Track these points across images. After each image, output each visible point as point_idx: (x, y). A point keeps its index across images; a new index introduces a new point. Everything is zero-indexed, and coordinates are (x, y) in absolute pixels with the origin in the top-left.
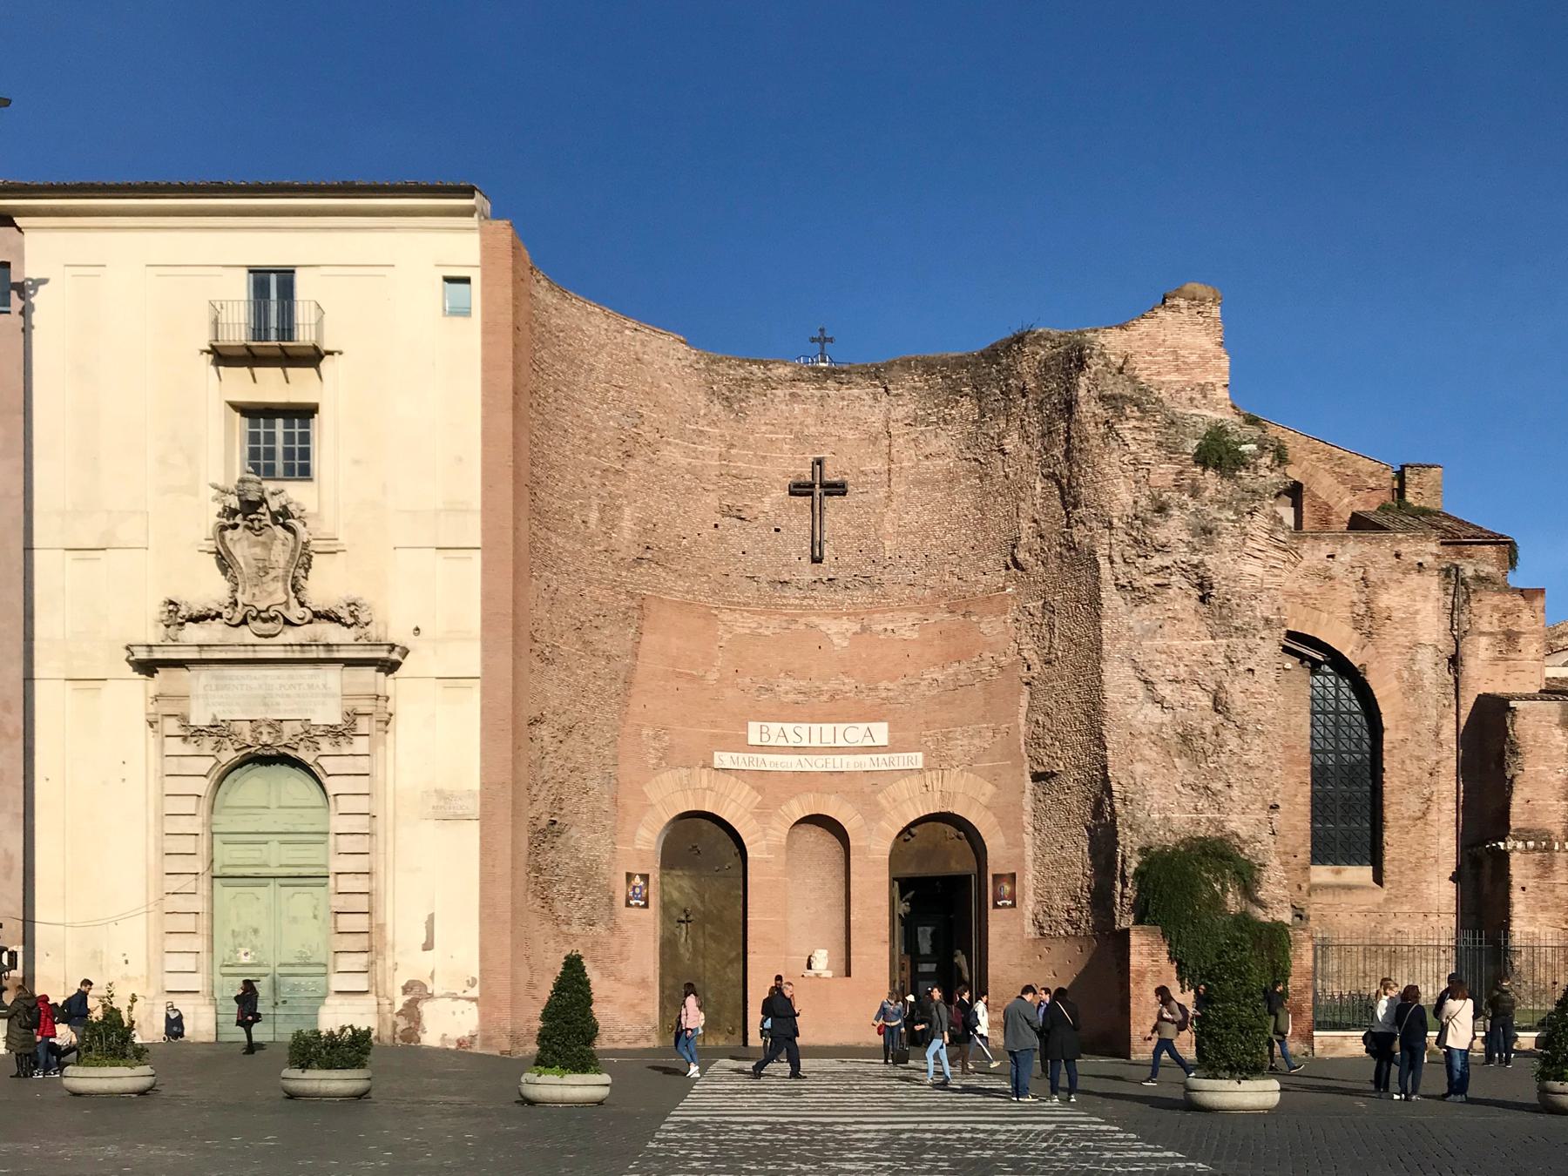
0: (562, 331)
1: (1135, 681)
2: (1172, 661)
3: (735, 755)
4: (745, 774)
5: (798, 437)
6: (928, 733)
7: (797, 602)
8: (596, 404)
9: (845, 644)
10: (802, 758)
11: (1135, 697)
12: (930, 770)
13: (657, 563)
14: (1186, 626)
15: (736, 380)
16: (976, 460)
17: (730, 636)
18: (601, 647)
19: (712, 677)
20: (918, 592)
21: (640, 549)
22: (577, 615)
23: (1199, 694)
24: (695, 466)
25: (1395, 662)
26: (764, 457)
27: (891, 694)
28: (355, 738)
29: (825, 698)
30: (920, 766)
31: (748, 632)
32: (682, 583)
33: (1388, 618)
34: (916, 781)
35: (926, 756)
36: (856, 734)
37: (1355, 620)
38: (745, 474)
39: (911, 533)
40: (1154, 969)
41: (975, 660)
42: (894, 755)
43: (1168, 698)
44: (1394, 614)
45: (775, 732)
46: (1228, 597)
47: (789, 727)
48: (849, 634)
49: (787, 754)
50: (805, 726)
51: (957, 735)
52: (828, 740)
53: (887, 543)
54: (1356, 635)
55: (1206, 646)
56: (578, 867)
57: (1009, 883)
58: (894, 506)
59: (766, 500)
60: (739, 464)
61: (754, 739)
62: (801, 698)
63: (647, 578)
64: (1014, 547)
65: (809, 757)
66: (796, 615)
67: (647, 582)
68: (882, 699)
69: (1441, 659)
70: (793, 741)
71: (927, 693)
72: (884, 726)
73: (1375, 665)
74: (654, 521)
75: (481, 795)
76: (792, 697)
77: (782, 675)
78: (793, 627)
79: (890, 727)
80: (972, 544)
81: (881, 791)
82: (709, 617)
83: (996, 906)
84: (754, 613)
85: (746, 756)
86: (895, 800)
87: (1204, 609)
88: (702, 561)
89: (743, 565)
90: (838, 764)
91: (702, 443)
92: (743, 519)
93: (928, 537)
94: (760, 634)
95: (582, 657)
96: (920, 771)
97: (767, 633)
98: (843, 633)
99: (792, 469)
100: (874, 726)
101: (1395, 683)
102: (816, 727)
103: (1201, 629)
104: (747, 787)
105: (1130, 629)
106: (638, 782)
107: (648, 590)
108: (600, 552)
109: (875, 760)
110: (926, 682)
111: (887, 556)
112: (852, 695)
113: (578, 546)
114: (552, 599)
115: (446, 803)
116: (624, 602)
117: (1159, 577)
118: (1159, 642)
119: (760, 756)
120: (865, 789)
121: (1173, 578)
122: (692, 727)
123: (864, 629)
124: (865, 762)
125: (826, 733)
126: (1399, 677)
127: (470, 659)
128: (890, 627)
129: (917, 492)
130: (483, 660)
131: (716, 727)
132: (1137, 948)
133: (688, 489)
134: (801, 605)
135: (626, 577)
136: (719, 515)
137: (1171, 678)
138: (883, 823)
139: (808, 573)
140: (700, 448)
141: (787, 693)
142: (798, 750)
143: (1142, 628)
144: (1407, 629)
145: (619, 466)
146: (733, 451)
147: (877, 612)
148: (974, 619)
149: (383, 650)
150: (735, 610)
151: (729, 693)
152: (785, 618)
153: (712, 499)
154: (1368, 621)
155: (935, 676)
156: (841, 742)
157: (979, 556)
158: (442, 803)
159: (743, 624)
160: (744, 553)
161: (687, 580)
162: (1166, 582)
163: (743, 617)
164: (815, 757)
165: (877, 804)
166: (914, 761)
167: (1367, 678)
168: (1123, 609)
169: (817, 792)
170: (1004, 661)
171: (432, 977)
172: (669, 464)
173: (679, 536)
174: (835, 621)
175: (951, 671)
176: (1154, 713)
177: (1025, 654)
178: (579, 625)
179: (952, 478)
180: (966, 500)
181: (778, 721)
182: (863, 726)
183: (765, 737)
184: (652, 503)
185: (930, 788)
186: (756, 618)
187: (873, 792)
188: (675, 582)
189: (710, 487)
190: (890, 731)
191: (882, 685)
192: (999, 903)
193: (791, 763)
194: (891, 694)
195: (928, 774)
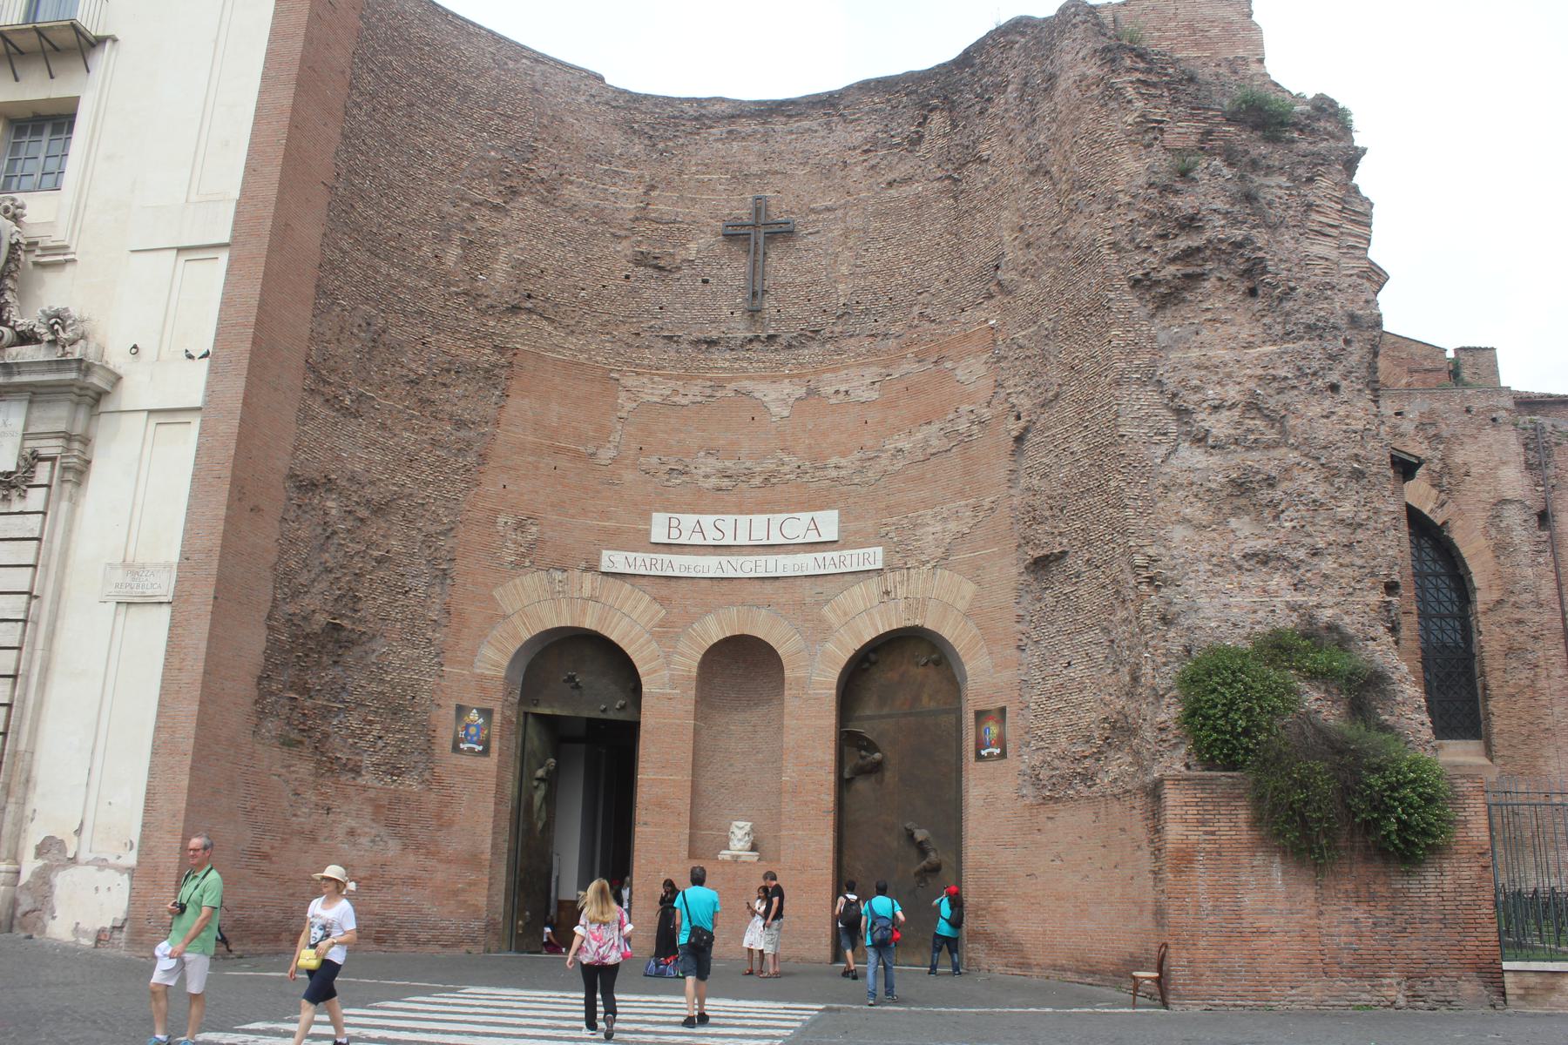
0: (428, 45)
1: (1164, 412)
2: (1215, 378)
3: (631, 555)
4: (644, 581)
5: (735, 177)
6: (889, 520)
7: (727, 364)
8: (473, 130)
9: (786, 413)
10: (724, 559)
11: (1165, 434)
12: (892, 570)
13: (541, 315)
14: (1233, 330)
15: (663, 119)
16: (949, 177)
17: (635, 405)
18: (448, 407)
19: (606, 455)
20: (880, 344)
21: (518, 296)
22: (414, 366)
23: (1260, 423)
24: (603, 210)
25: (1479, 518)
26: (692, 199)
27: (843, 473)
28: (30, 490)
29: (757, 481)
30: (879, 565)
31: (659, 400)
32: (575, 340)
33: (1467, 474)
34: (874, 586)
35: (887, 553)
36: (797, 526)
37: (1432, 478)
38: (666, 217)
39: (872, 273)
40: (1208, 847)
41: (951, 417)
42: (845, 552)
43: (1214, 431)
44: (1473, 470)
45: (687, 526)
46: (1292, 284)
47: (707, 520)
48: (791, 401)
49: (704, 555)
50: (730, 519)
51: (928, 519)
52: (759, 537)
53: (841, 287)
54: (1434, 492)
55: (1265, 355)
56: (382, 693)
57: (997, 722)
58: (850, 244)
59: (693, 246)
60: (661, 207)
61: (658, 534)
62: (726, 483)
63: (523, 331)
64: (997, 267)
65: (733, 559)
66: (725, 379)
67: (523, 335)
68: (833, 480)
69: (1530, 515)
70: (712, 538)
71: (890, 468)
72: (833, 515)
73: (1459, 523)
74: (542, 266)
75: (179, 567)
76: (713, 482)
77: (702, 453)
78: (719, 394)
79: (840, 515)
80: (946, 276)
81: (827, 602)
82: (609, 382)
83: (979, 757)
84: (669, 377)
85: (648, 557)
86: (845, 614)
87: (1258, 305)
88: (606, 317)
89: (659, 322)
90: (771, 566)
91: (615, 184)
92: (661, 269)
93: (893, 276)
94: (675, 404)
95: (413, 416)
96: (879, 571)
97: (684, 401)
98: (784, 400)
99: (727, 211)
100: (820, 516)
101: (1483, 542)
102: (743, 520)
103: (1256, 331)
104: (647, 598)
105: (1153, 339)
106: (486, 585)
107: (524, 344)
108: (457, 294)
109: (820, 561)
110: (889, 454)
111: (842, 300)
112: (793, 477)
113: (425, 283)
114: (374, 341)
115: (134, 579)
116: (488, 356)
117: (1188, 265)
118: (1194, 354)
119: (667, 557)
120: (808, 600)
121: (1209, 266)
122: (573, 517)
123: (812, 392)
124: (807, 563)
125: (759, 527)
126: (1486, 533)
127: (191, 384)
128: (843, 389)
129: (878, 224)
130: (209, 385)
131: (610, 519)
132: (1178, 811)
133: (593, 234)
134: (731, 369)
135: (494, 327)
136: (631, 265)
137: (1217, 403)
138: (830, 646)
139: (741, 331)
140: (613, 189)
141: (707, 477)
142: (717, 549)
143: (1171, 338)
144: (1489, 485)
145: (499, 201)
146: (652, 194)
147: (828, 370)
148: (949, 365)
149: (71, 370)
150: (643, 374)
151: (628, 476)
152: (709, 383)
153: (625, 247)
155: (899, 445)
156: (776, 539)
157: (956, 288)
158: (128, 580)
159: (654, 391)
160: (661, 308)
161: (581, 337)
162: (1198, 270)
163: (654, 383)
164: (741, 559)
165: (821, 620)
166: (871, 559)
167: (1451, 536)
168: (1141, 312)
169: (743, 604)
170: (986, 413)
171: (78, 832)
172: (569, 205)
173: (576, 287)
174: (774, 386)
175: (919, 436)
176: (1192, 457)
177: (1013, 400)
178: (412, 376)
179: (920, 204)
180: (939, 226)
181: (694, 513)
182: (805, 517)
183: (675, 533)
184: (540, 246)
185: (893, 595)
186: (672, 384)
187: (817, 603)
188: (563, 338)
189: (623, 233)
190: (840, 521)
191: (834, 460)
192: (984, 753)
193: (709, 566)
194: (843, 473)
195: (890, 575)
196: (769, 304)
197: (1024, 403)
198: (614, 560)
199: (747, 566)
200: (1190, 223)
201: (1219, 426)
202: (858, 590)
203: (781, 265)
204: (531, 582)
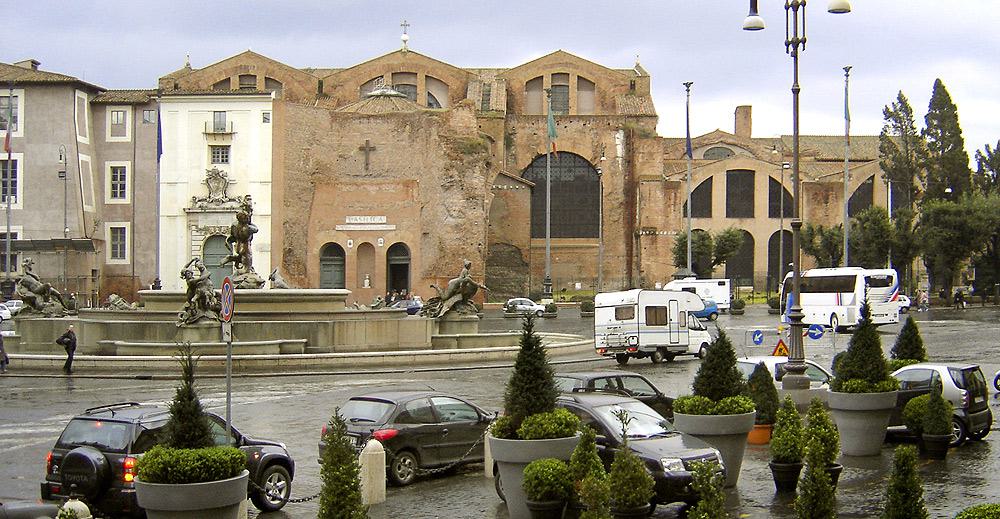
36: (377, 219)
52: (369, 221)
61: (347, 221)
124: (380, 227)
126: (610, 169)
154: (599, 150)
176: (451, 219)
193: (358, 228)
196: (370, 167)
197: (423, 201)
198: (339, 228)
199: (368, 228)
200: (451, 177)
201: (455, 214)
202: (390, 234)
203: (372, 157)
204: (323, 233)
